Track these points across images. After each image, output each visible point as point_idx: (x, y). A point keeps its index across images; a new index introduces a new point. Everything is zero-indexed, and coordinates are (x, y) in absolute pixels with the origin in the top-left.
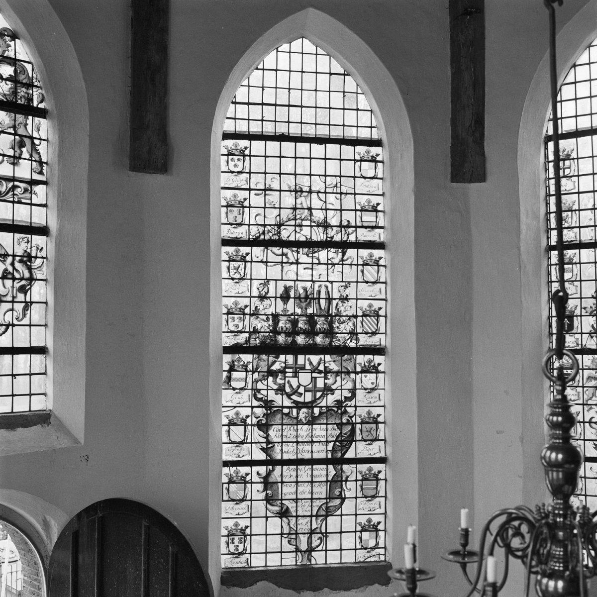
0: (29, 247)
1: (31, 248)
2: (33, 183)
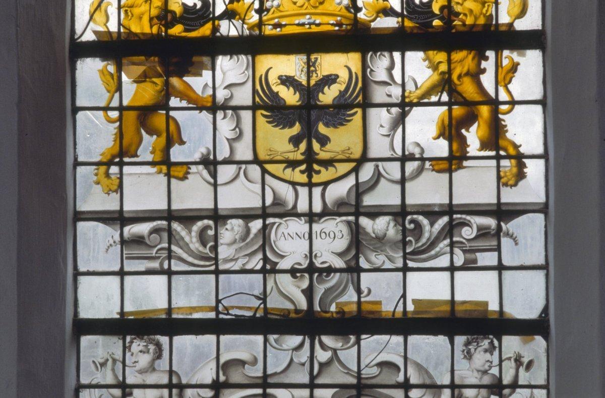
0: (496, 361)
1: (500, 365)
2: (504, 212)
